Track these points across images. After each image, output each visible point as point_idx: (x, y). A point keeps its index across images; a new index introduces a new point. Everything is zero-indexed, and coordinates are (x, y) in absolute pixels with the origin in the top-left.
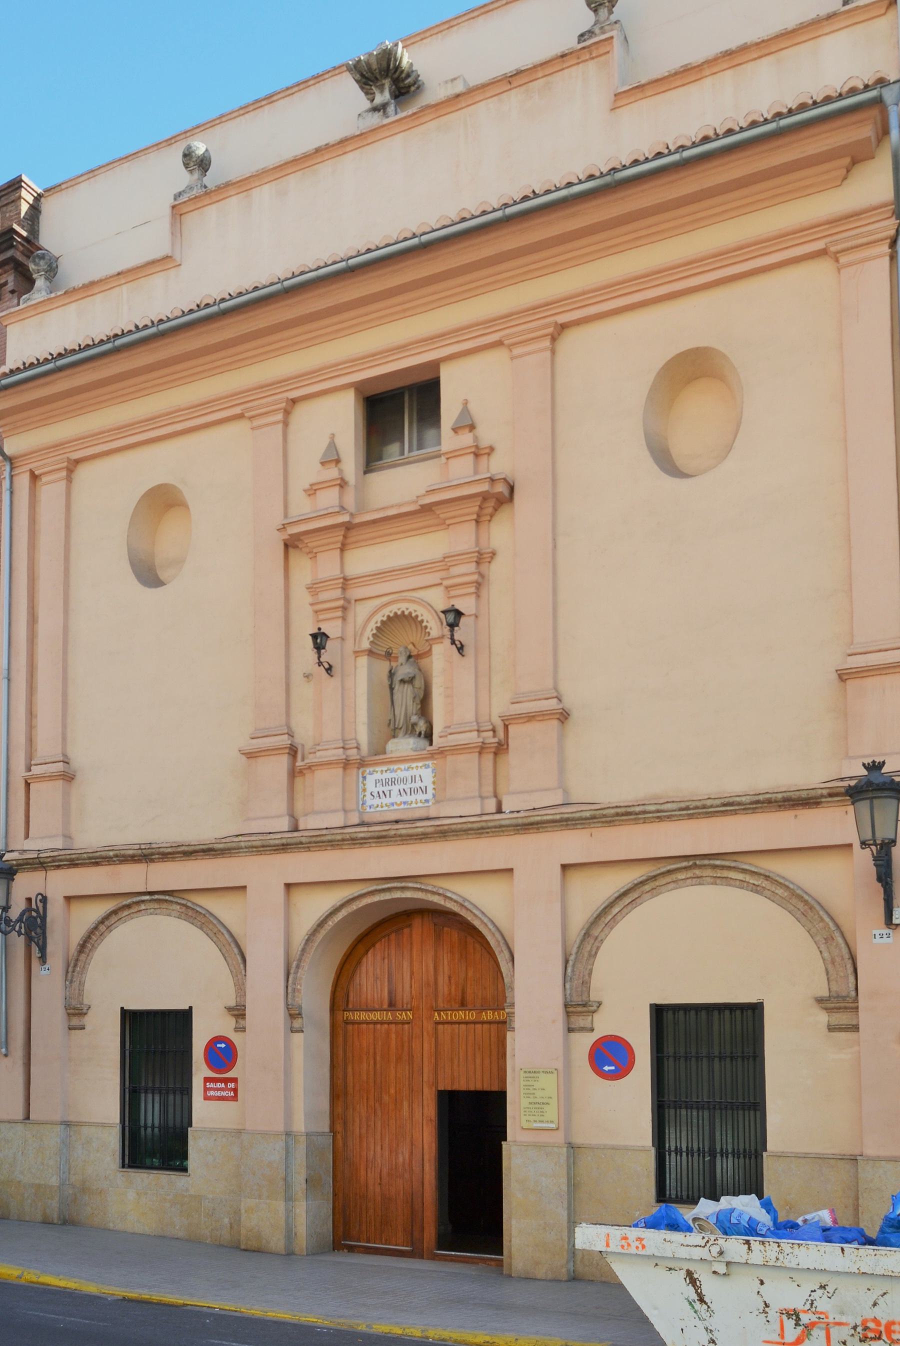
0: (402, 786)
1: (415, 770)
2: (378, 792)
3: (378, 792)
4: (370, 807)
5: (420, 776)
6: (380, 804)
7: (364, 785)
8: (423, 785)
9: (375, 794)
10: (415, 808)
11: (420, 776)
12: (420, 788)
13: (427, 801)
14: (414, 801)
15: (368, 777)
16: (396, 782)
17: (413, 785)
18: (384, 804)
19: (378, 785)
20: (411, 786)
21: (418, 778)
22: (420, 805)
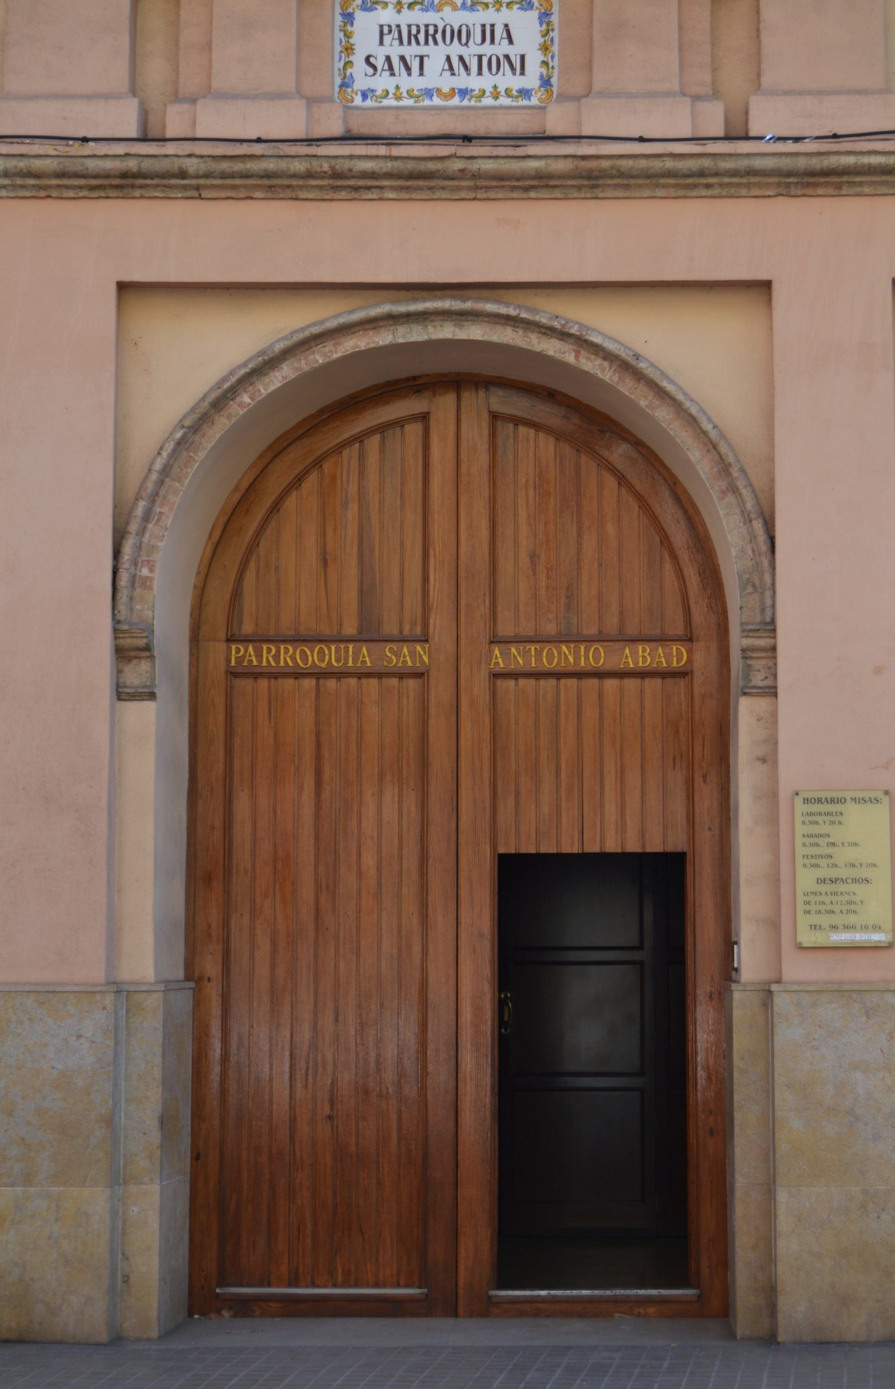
0: (455, 49)
1: (491, 10)
2: (388, 59)
3: (388, 59)
4: (365, 96)
5: (506, 25)
6: (392, 90)
7: (348, 35)
8: (514, 52)
9: (380, 63)
10: (493, 108)
11: (506, 25)
12: (507, 57)
13: (524, 93)
14: (489, 90)
15: (360, 16)
16: (439, 36)
17: (487, 49)
18: (404, 90)
19: (387, 39)
20: (481, 50)
21: (499, 32)
22: (504, 101)
